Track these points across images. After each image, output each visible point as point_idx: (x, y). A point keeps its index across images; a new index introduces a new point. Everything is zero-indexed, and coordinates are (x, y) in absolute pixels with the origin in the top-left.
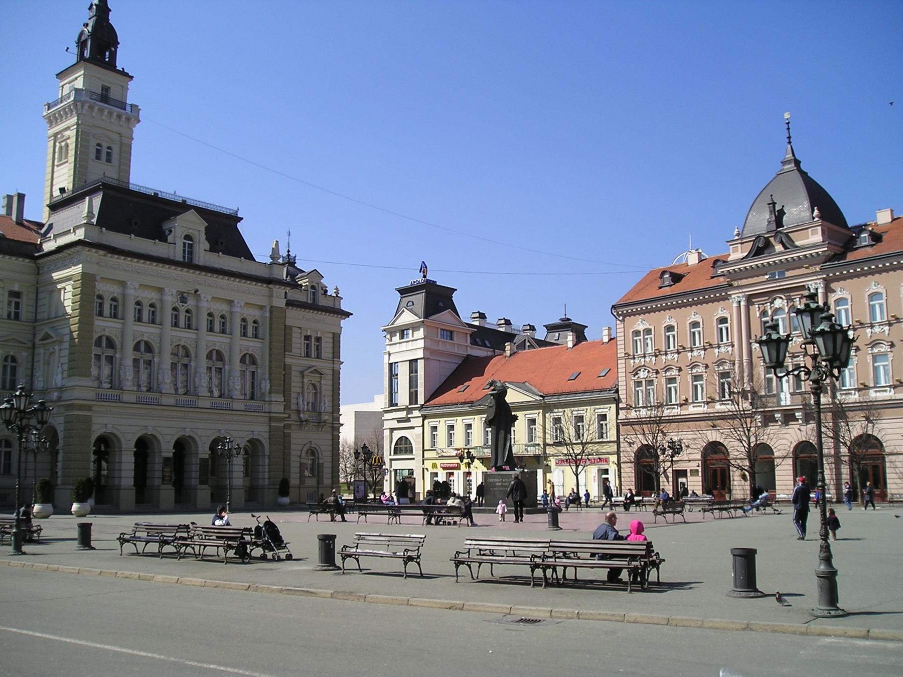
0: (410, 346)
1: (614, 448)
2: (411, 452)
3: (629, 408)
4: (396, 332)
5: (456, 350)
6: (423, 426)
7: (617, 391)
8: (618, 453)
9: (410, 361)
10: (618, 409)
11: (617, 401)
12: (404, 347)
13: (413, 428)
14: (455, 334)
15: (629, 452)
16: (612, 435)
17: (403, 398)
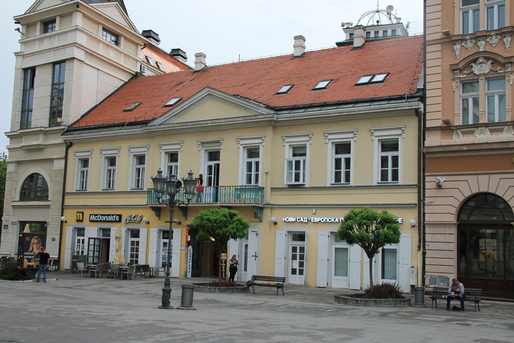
0: (57, 42)
1: (412, 197)
2: (45, 198)
3: (447, 128)
4: (34, 24)
5: (121, 61)
6: (66, 158)
7: (423, 99)
8: (420, 205)
9: (54, 64)
10: (423, 131)
11: (420, 116)
12: (47, 44)
13: (51, 160)
14: (122, 40)
15: (444, 209)
16: (408, 172)
17: (40, 117)
